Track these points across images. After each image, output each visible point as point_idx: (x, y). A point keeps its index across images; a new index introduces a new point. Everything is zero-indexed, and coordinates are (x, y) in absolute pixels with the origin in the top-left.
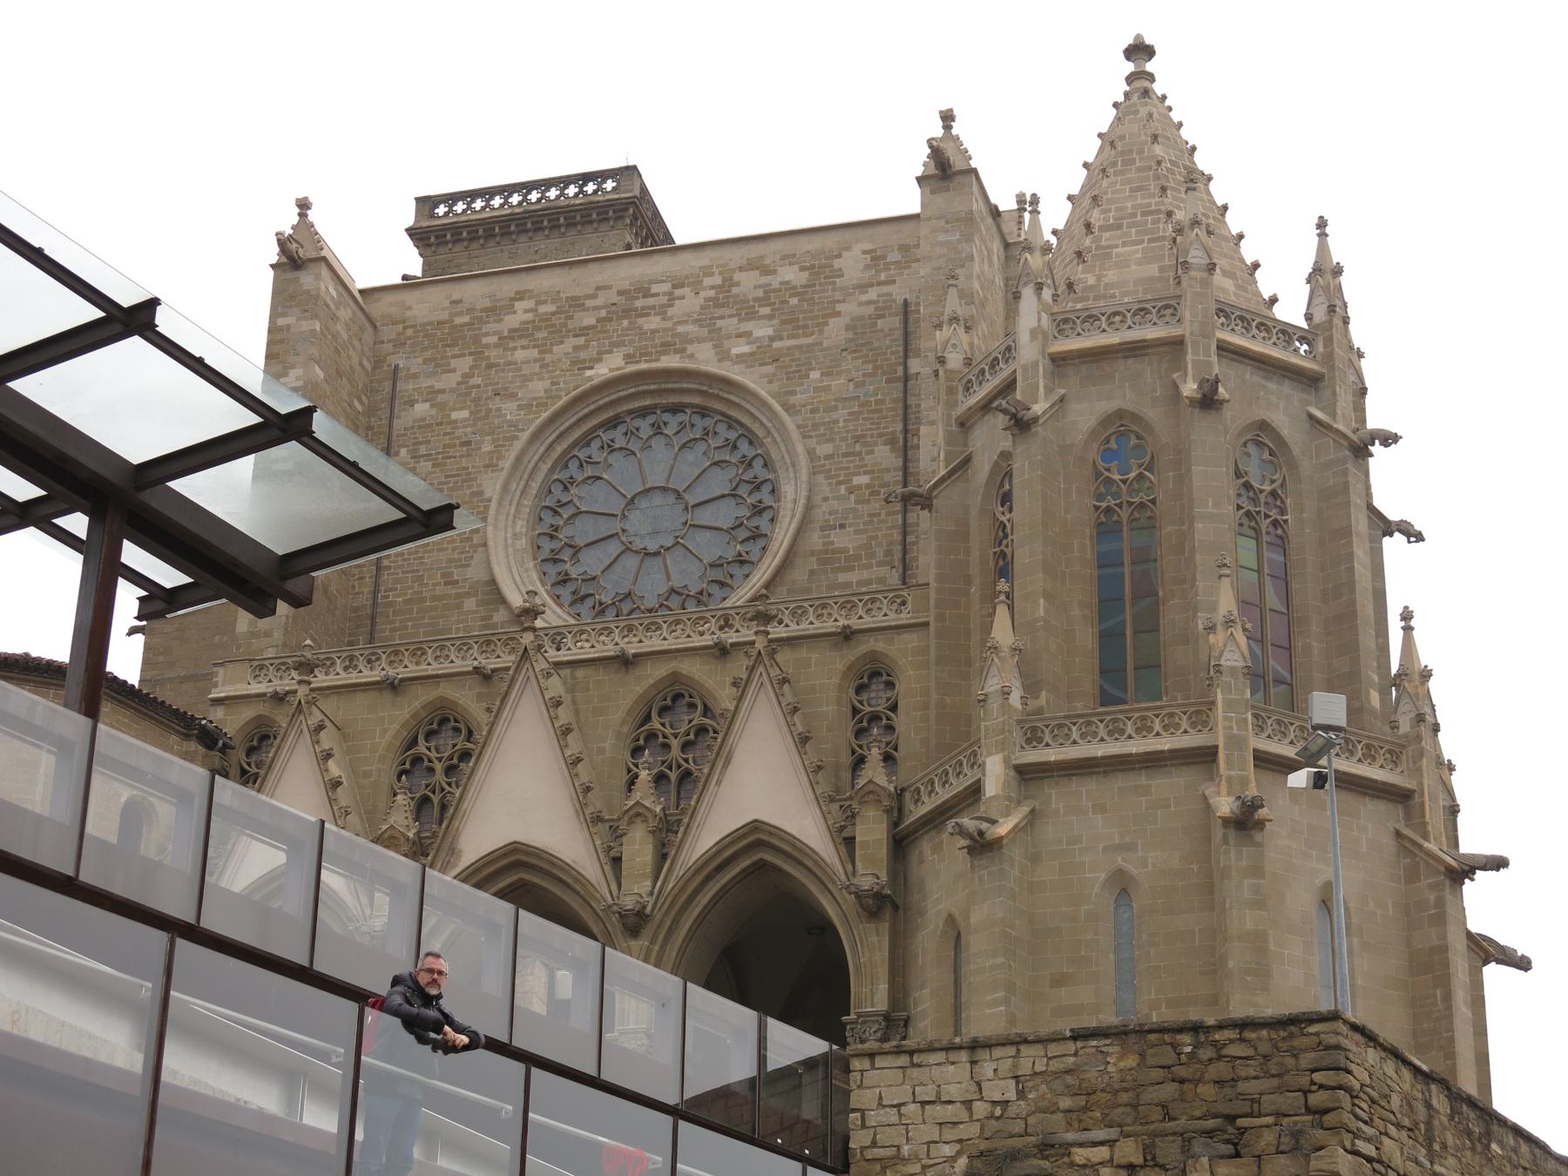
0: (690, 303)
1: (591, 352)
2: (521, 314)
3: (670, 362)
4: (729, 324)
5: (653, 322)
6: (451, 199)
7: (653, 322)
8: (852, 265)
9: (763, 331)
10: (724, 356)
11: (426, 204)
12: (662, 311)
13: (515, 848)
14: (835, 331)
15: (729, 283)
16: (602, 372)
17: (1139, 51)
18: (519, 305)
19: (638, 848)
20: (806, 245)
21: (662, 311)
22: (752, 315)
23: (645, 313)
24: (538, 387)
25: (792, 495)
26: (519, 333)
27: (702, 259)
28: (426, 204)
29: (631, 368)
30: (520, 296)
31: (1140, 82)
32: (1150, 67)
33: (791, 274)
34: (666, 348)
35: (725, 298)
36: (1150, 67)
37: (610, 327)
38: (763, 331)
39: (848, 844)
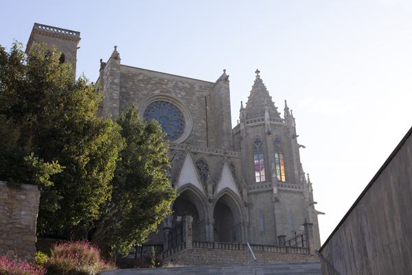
0: (171, 85)
1: (154, 88)
2: (141, 77)
3: (168, 94)
4: (177, 91)
5: (164, 86)
6: (42, 26)
7: (164, 86)
8: (197, 87)
9: (183, 94)
10: (177, 96)
11: (36, 25)
12: (166, 85)
13: (190, 184)
14: (194, 97)
15: (176, 84)
16: (157, 92)
17: (258, 72)
18: (141, 76)
19: (210, 188)
20: (189, 81)
21: (166, 85)
22: (181, 90)
23: (163, 84)
24: (146, 92)
25: (189, 124)
26: (141, 80)
27: (173, 77)
28: (36, 25)
29: (161, 94)
30: (141, 74)
31: (258, 76)
32: (259, 74)
33: (187, 85)
34: (167, 92)
35: (176, 86)
36: (259, 74)
37: (157, 85)
38: (183, 94)
39: (241, 193)
